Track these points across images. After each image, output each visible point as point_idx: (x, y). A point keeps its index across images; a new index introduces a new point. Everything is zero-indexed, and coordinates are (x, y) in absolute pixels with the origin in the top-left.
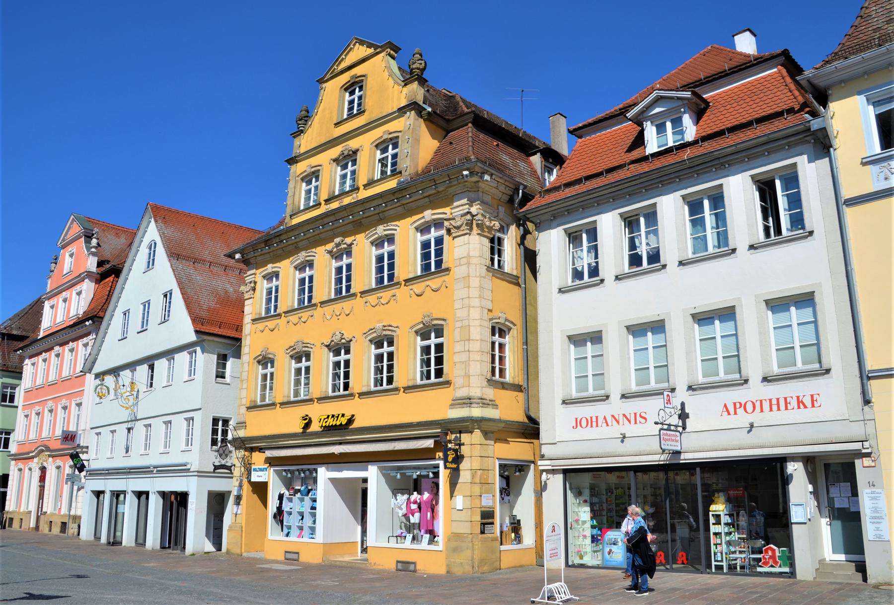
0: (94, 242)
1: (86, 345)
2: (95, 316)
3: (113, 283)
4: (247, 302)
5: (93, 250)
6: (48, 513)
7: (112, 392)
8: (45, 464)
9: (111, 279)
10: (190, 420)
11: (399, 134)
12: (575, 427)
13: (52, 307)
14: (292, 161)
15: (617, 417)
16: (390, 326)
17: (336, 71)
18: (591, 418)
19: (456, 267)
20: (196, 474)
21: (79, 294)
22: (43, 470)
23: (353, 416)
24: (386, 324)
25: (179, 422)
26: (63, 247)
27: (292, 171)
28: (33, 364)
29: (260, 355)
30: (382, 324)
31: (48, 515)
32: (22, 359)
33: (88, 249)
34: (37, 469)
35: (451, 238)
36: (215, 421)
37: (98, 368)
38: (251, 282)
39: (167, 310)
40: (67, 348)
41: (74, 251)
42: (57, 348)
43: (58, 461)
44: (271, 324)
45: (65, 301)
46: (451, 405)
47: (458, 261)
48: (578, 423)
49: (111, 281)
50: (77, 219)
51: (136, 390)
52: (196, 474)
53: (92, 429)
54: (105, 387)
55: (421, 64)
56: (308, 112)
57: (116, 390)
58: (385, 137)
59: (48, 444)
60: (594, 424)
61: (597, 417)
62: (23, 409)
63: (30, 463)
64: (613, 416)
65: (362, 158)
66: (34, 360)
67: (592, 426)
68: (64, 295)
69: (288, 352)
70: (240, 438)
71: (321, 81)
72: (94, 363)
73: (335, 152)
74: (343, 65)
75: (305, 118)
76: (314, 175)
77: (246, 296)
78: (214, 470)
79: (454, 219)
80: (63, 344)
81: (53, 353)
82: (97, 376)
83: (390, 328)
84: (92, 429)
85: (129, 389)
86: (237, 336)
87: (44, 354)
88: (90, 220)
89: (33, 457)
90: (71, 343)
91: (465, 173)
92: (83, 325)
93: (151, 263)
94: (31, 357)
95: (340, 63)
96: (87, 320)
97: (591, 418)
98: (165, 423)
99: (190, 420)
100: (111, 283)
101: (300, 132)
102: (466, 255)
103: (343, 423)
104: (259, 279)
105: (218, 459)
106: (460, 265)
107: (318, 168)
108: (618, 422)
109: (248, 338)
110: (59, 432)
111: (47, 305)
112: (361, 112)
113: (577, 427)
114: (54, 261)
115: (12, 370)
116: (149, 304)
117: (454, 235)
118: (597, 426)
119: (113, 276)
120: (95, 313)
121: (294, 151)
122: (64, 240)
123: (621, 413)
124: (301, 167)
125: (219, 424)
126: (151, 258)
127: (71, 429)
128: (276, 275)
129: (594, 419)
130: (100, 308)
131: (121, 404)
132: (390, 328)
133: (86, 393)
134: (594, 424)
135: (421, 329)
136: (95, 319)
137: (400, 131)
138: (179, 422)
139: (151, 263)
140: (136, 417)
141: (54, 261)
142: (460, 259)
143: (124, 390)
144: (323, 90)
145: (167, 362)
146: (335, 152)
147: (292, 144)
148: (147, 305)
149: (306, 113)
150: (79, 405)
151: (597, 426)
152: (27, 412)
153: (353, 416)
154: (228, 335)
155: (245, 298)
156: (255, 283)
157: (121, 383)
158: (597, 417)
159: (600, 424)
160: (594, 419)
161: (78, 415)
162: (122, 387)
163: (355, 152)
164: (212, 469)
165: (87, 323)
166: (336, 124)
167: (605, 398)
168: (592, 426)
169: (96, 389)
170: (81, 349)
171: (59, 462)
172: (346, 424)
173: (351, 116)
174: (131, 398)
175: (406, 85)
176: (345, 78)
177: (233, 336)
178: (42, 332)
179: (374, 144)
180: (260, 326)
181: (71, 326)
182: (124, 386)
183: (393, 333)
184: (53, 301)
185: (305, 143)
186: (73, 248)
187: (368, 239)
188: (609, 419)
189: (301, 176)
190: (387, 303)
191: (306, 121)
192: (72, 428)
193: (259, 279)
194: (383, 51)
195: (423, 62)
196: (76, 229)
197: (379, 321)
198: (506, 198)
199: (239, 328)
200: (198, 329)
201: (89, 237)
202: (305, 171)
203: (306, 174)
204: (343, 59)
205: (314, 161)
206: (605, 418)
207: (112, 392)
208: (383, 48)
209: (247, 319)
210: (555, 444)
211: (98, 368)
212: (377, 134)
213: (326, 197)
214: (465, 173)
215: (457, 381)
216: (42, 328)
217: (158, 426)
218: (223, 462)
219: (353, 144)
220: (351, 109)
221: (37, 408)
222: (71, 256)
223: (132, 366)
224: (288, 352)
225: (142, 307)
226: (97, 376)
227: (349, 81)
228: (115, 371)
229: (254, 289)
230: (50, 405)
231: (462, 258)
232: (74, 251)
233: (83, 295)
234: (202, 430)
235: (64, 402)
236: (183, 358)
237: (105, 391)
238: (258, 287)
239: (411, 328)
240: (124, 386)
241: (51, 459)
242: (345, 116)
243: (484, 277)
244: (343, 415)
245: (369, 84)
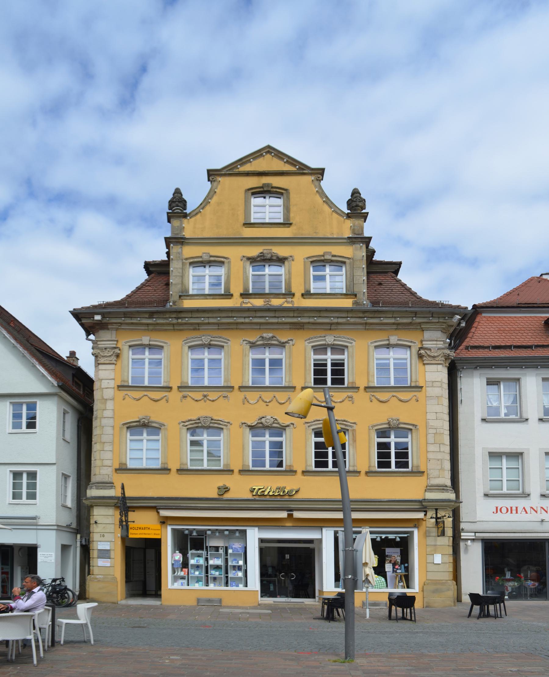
12: (495, 512)
15: (536, 509)
18: (511, 508)
19: (428, 387)
47: (431, 383)
48: (498, 510)
60: (514, 512)
61: (517, 508)
64: (531, 508)
67: (511, 512)
97: (511, 508)
102: (440, 380)
108: (536, 512)
109: (110, 405)
113: (497, 512)
118: (517, 512)
123: (539, 506)
129: (514, 509)
134: (514, 512)
142: (433, 382)
151: (517, 512)
158: (517, 508)
159: (519, 511)
160: (514, 509)
167: (527, 495)
168: (511, 512)
188: (528, 510)
206: (524, 508)
210: (476, 522)
231: (435, 381)
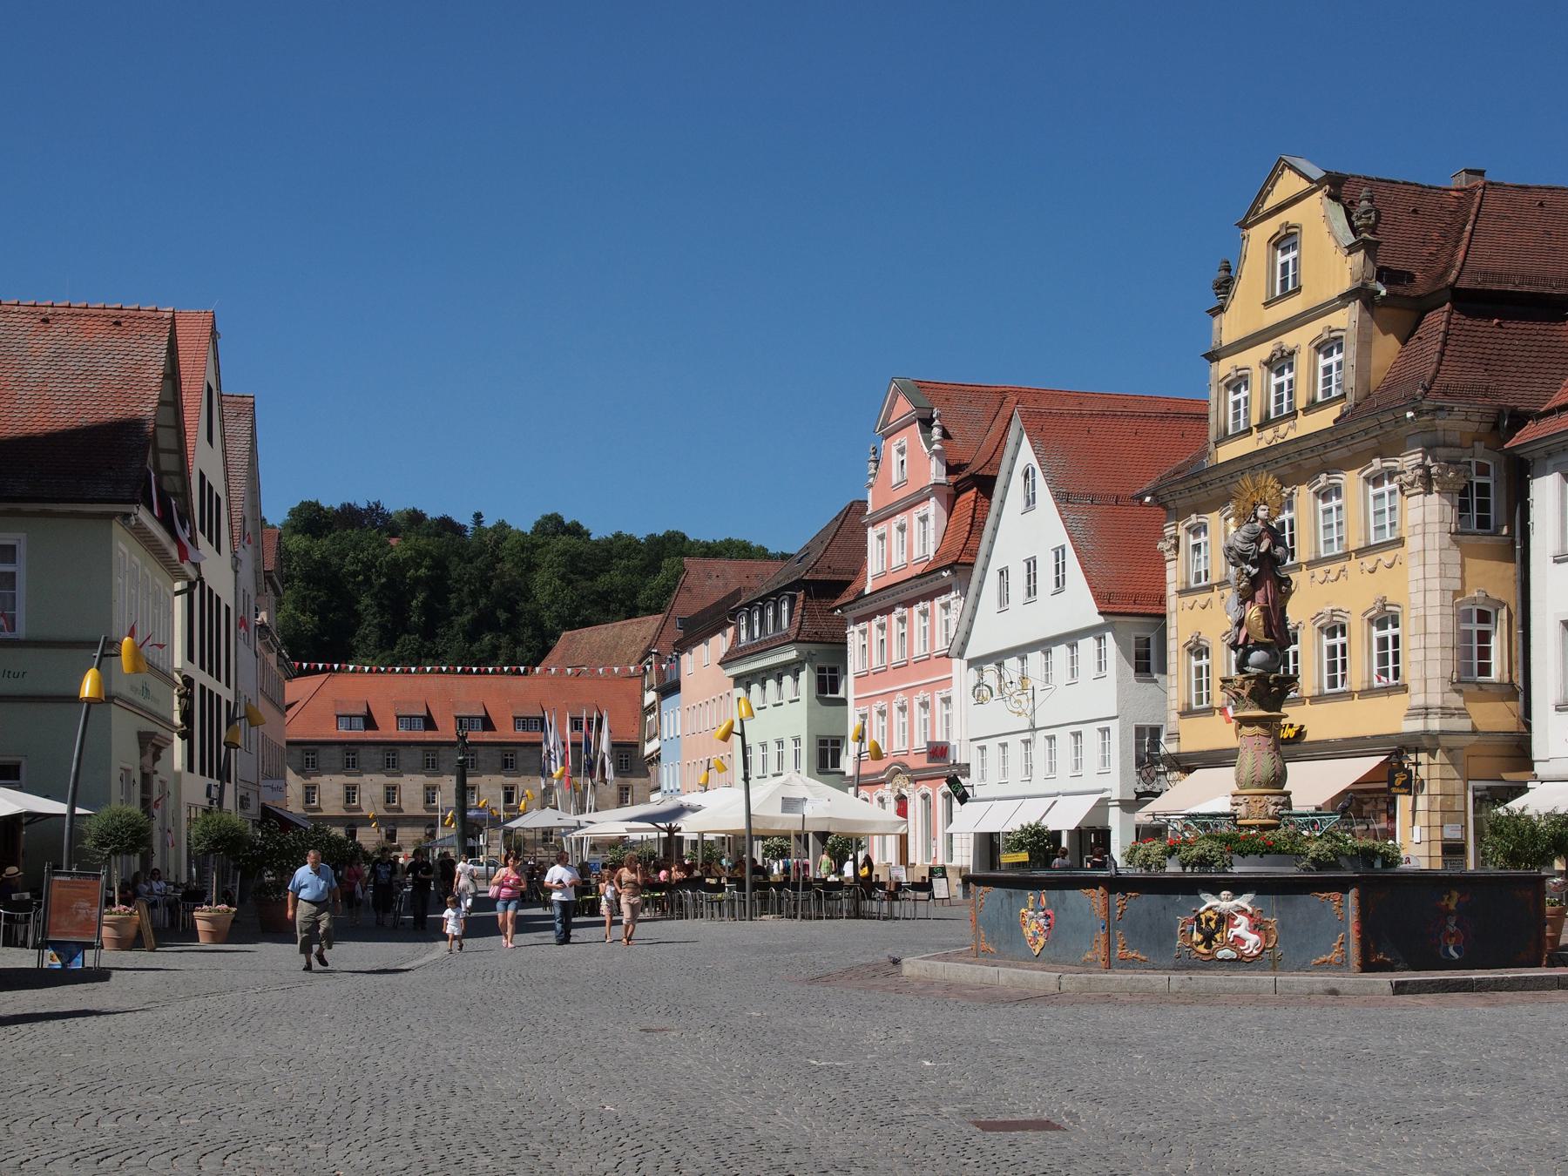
0: (936, 433)
1: (946, 606)
2: (956, 563)
3: (975, 502)
4: (1169, 565)
5: (936, 447)
6: (918, 864)
7: (996, 692)
8: (904, 792)
9: (971, 494)
10: (1105, 731)
11: (1343, 334)
13: (881, 537)
14: (1213, 356)
16: (1340, 610)
17: (1261, 211)
20: (1117, 803)
21: (924, 519)
22: (902, 801)
23: (1302, 727)
24: (1335, 608)
25: (1091, 733)
26: (887, 436)
27: (1212, 371)
28: (863, 632)
29: (1191, 642)
30: (1330, 608)
31: (919, 868)
32: (843, 624)
33: (929, 443)
34: (893, 800)
35: (1405, 498)
36: (1140, 731)
37: (972, 652)
38: (1171, 537)
39: (1060, 568)
40: (916, 609)
41: (905, 443)
42: (899, 610)
43: (923, 786)
44: (1202, 598)
45: (902, 529)
46: (1407, 715)
49: (973, 498)
50: (903, 389)
51: (1030, 687)
52: (1117, 803)
53: (971, 740)
54: (985, 688)
55: (1370, 218)
56: (1228, 270)
57: (1001, 691)
58: (1326, 336)
59: (906, 760)
62: (856, 706)
63: (880, 790)
65: (1301, 361)
66: (862, 626)
68: (899, 521)
69: (1224, 638)
70: (1169, 754)
71: (1245, 225)
72: (964, 644)
73: (1265, 350)
74: (1271, 202)
75: (1225, 286)
76: (1238, 382)
77: (1168, 556)
78: (1137, 798)
79: (1404, 472)
80: (909, 603)
81: (894, 617)
82: (972, 663)
83: (1340, 613)
84: (971, 740)
85: (1020, 687)
86: (1161, 612)
87: (878, 617)
88: (921, 386)
89: (883, 782)
90: (921, 604)
91: (1409, 414)
92: (937, 575)
93: (1030, 501)
94: (857, 621)
95: (1263, 203)
96: (944, 568)
98: (1073, 734)
99: (1105, 731)
100: (972, 504)
101: (1221, 309)
103: (1291, 736)
104: (1181, 532)
105: (1141, 785)
106: (1414, 535)
107: (1246, 371)
109: (1174, 615)
110: (920, 744)
111: (872, 534)
112: (1298, 290)
114: (872, 457)
115: (829, 640)
116: (1035, 562)
117: (1407, 493)
119: (975, 489)
120: (955, 558)
121: (1215, 338)
122: (885, 424)
124: (1225, 367)
125: (1148, 737)
126: (1032, 571)
127: (938, 739)
128: (1204, 528)
130: (961, 547)
131: (1011, 708)
132: (1340, 613)
133: (955, 681)
135: (1376, 615)
136: (956, 567)
137: (1344, 330)
138: (1091, 733)
139: (1030, 501)
140: (1033, 724)
141: (872, 457)
143: (1013, 690)
144: (1245, 241)
145: (1069, 650)
146: (1265, 350)
147: (1210, 325)
148: (1031, 564)
149: (1227, 274)
150: (947, 701)
152: (864, 709)
153: (1302, 727)
154: (1148, 611)
155: (1166, 559)
156: (1177, 538)
157: (1007, 680)
161: (947, 716)
162: (1009, 685)
163: (1292, 353)
164: (1133, 797)
165: (944, 574)
166: (1265, 304)
169: (974, 690)
170: (943, 615)
171: (925, 787)
172: (1295, 736)
173: (1286, 294)
174: (1023, 698)
175: (1350, 253)
176: (1270, 227)
177: (1155, 611)
178: (870, 579)
179: (1313, 345)
180: (1189, 600)
181: (919, 577)
182: (1011, 683)
183: (1345, 621)
184: (881, 528)
185: (1230, 327)
186: (901, 439)
187: (1310, 488)
189: (1225, 381)
190: (1336, 580)
191: (1228, 288)
192: (940, 737)
193: (1181, 532)
194: (1320, 188)
195: (1373, 214)
196: (903, 407)
197: (1328, 604)
198: (1484, 428)
199: (1162, 600)
200: (1103, 610)
201: (926, 424)
202: (1229, 375)
203: (1230, 378)
204: (1269, 192)
205: (1241, 359)
207: (996, 692)
208: (1319, 184)
209: (1171, 590)
211: (972, 652)
212: (1315, 329)
213: (1257, 422)
214: (1409, 414)
215: (1414, 686)
216: (869, 574)
217: (1063, 736)
218: (1148, 788)
219: (1289, 340)
220: (1284, 282)
221: (879, 703)
222: (901, 451)
223: (1021, 651)
224: (1224, 638)
225: (1025, 565)
226: (972, 663)
227: (1278, 233)
228: (998, 658)
229: (1177, 547)
230: (900, 700)
232: (905, 443)
233: (932, 519)
234: (1120, 749)
235: (922, 695)
236: (1087, 645)
237: (986, 692)
238: (1182, 541)
239: (1364, 615)
240: (1011, 683)
241: (912, 785)
242: (1278, 293)
243: (1449, 549)
244: (1291, 726)
245: (1306, 239)
